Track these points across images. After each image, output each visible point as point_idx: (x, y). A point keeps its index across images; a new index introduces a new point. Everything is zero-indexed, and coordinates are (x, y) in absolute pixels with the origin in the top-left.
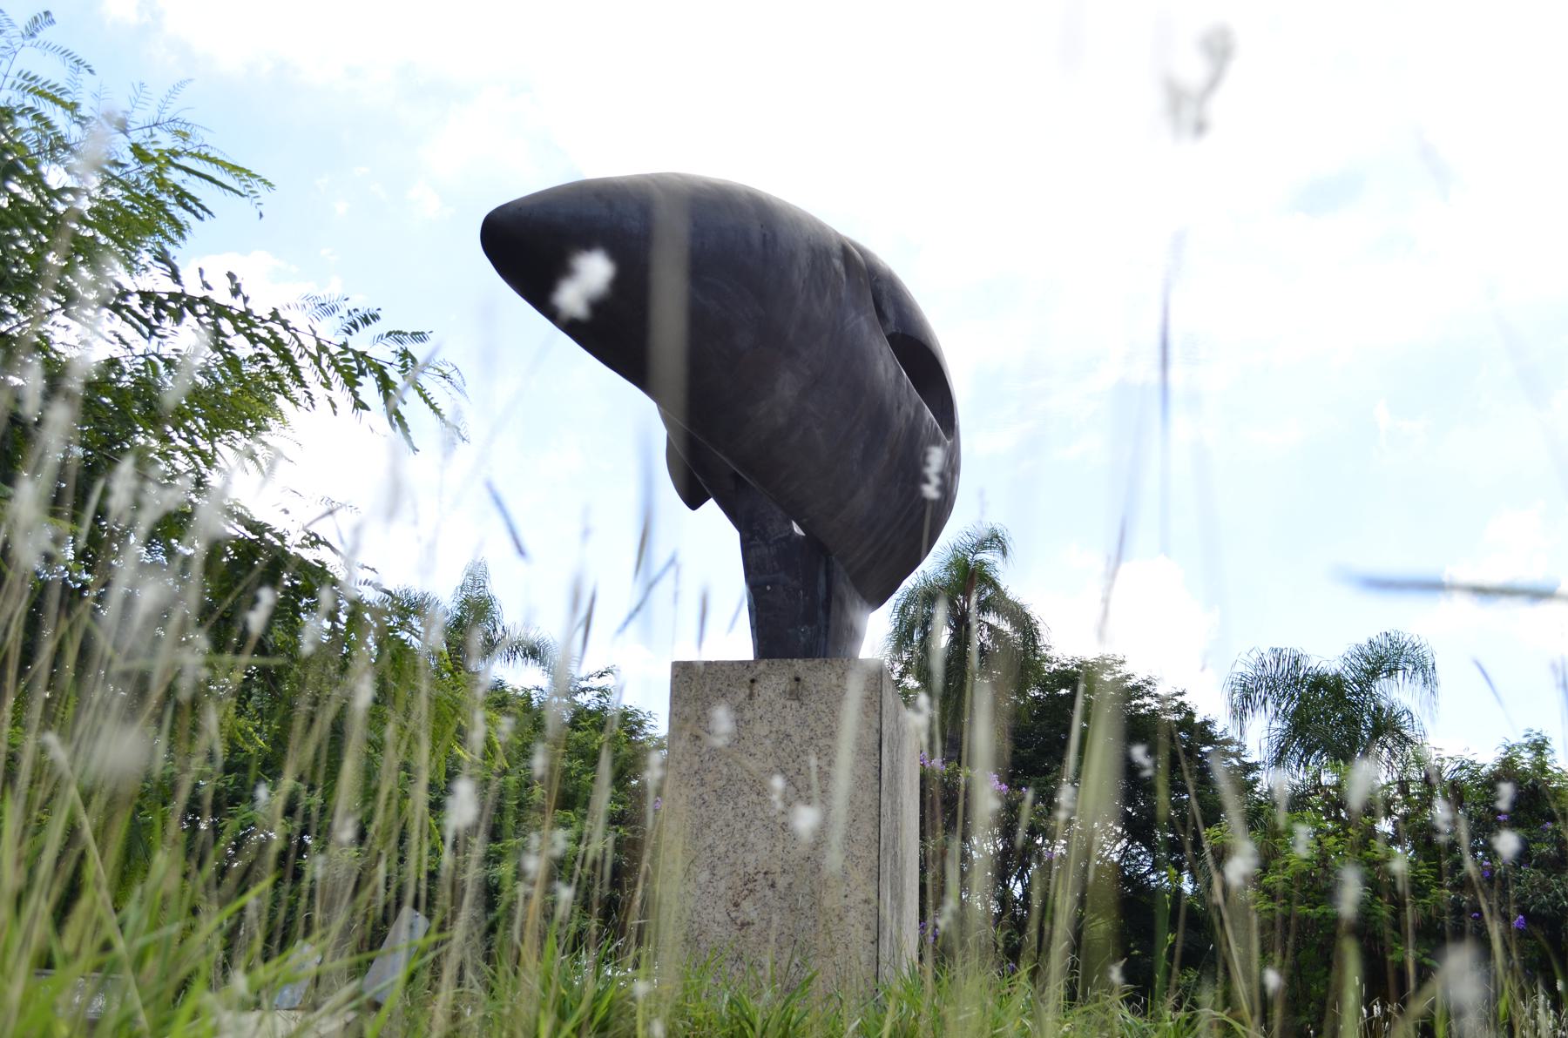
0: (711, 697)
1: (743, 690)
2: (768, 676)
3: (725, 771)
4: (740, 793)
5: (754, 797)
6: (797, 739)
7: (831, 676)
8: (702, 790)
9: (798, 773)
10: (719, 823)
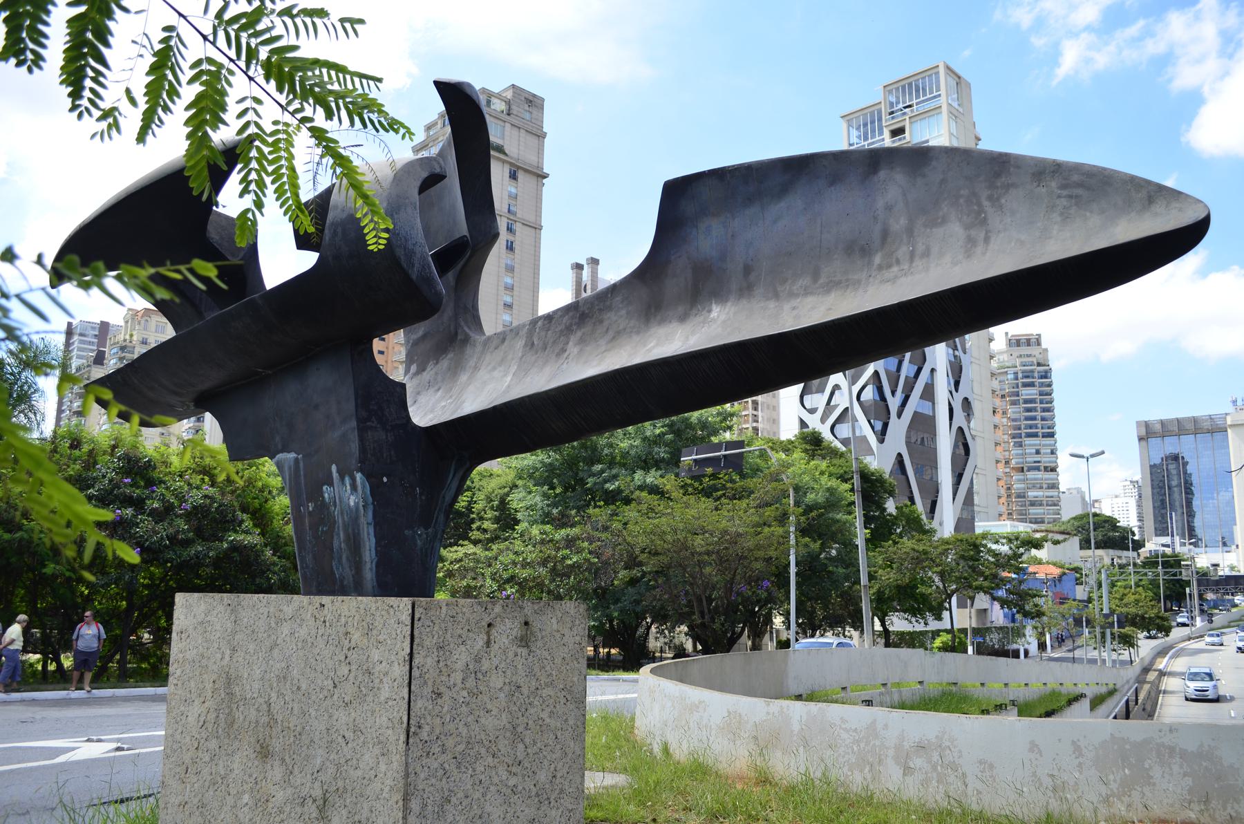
0: (452, 646)
1: (481, 636)
3: (464, 731)
4: (478, 756)
5: (490, 759)
6: (525, 691)
8: (443, 758)
9: (526, 729)
10: (459, 795)
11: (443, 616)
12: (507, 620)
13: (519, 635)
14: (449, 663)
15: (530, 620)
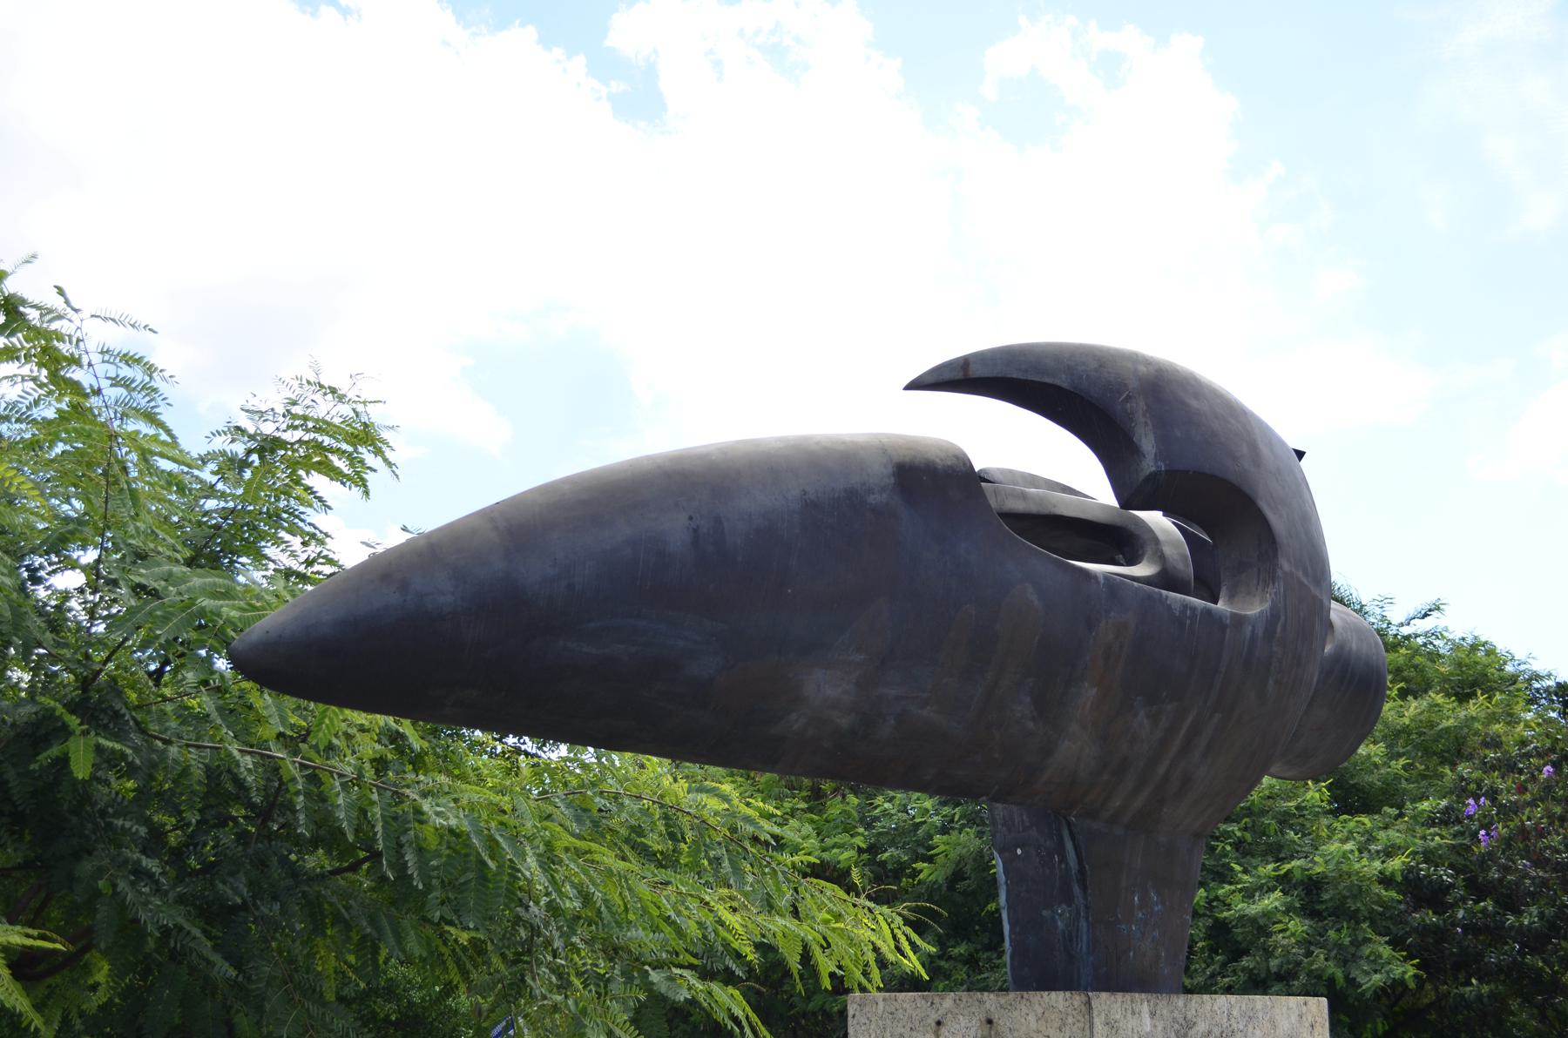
2: (955, 1016)
7: (1029, 1018)
11: (880, 1012)
12: (961, 1017)
15: (995, 1017)
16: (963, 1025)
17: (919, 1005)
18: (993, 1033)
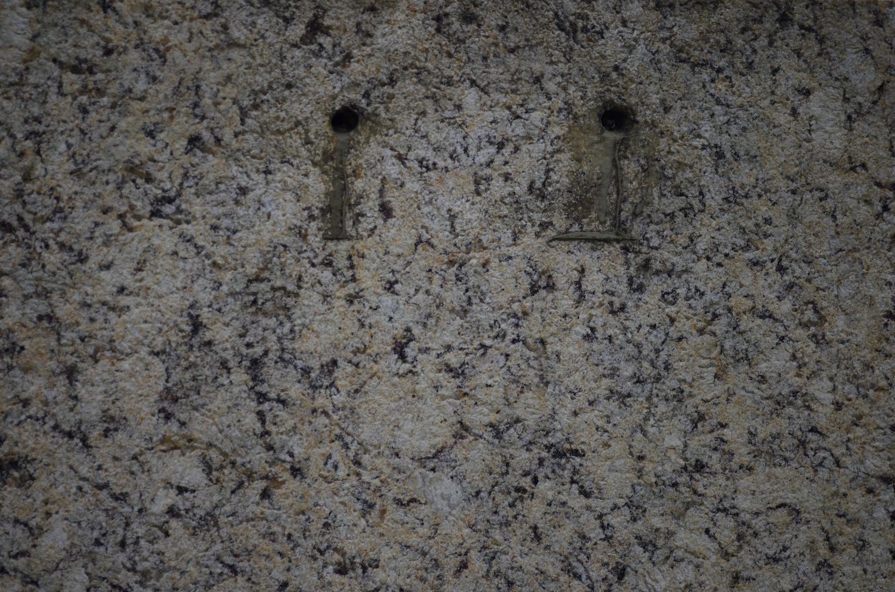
1: (285, 174)
7: (814, 106)
12: (471, 98)
13: (561, 178)
14: (63, 311)
16: (477, 131)
17: (238, 33)
18: (630, 167)
